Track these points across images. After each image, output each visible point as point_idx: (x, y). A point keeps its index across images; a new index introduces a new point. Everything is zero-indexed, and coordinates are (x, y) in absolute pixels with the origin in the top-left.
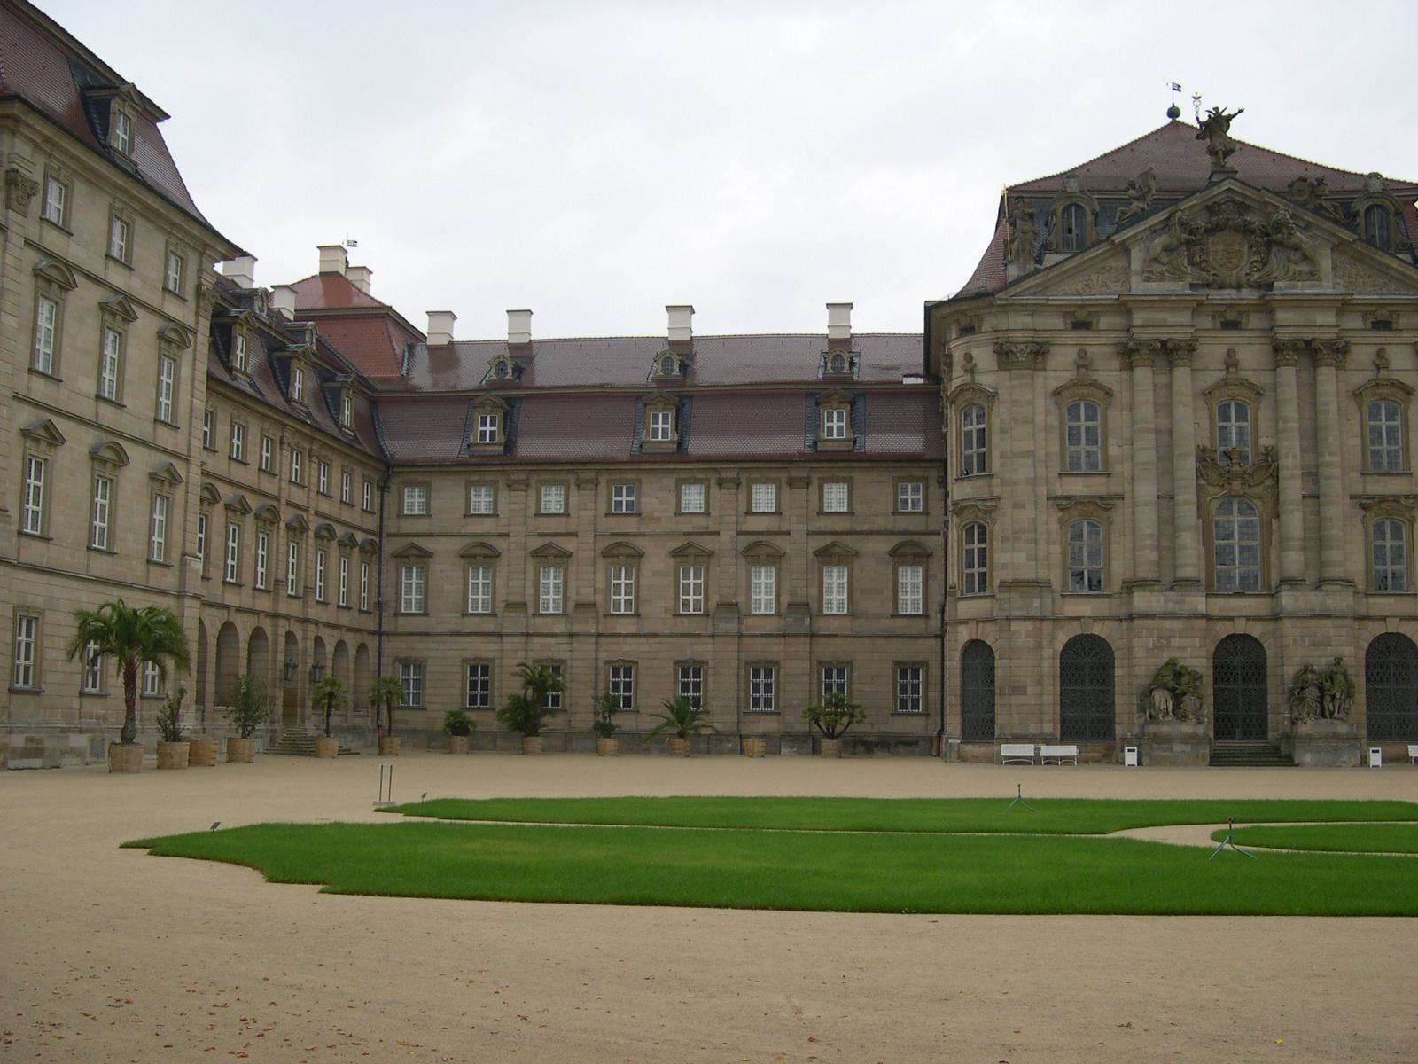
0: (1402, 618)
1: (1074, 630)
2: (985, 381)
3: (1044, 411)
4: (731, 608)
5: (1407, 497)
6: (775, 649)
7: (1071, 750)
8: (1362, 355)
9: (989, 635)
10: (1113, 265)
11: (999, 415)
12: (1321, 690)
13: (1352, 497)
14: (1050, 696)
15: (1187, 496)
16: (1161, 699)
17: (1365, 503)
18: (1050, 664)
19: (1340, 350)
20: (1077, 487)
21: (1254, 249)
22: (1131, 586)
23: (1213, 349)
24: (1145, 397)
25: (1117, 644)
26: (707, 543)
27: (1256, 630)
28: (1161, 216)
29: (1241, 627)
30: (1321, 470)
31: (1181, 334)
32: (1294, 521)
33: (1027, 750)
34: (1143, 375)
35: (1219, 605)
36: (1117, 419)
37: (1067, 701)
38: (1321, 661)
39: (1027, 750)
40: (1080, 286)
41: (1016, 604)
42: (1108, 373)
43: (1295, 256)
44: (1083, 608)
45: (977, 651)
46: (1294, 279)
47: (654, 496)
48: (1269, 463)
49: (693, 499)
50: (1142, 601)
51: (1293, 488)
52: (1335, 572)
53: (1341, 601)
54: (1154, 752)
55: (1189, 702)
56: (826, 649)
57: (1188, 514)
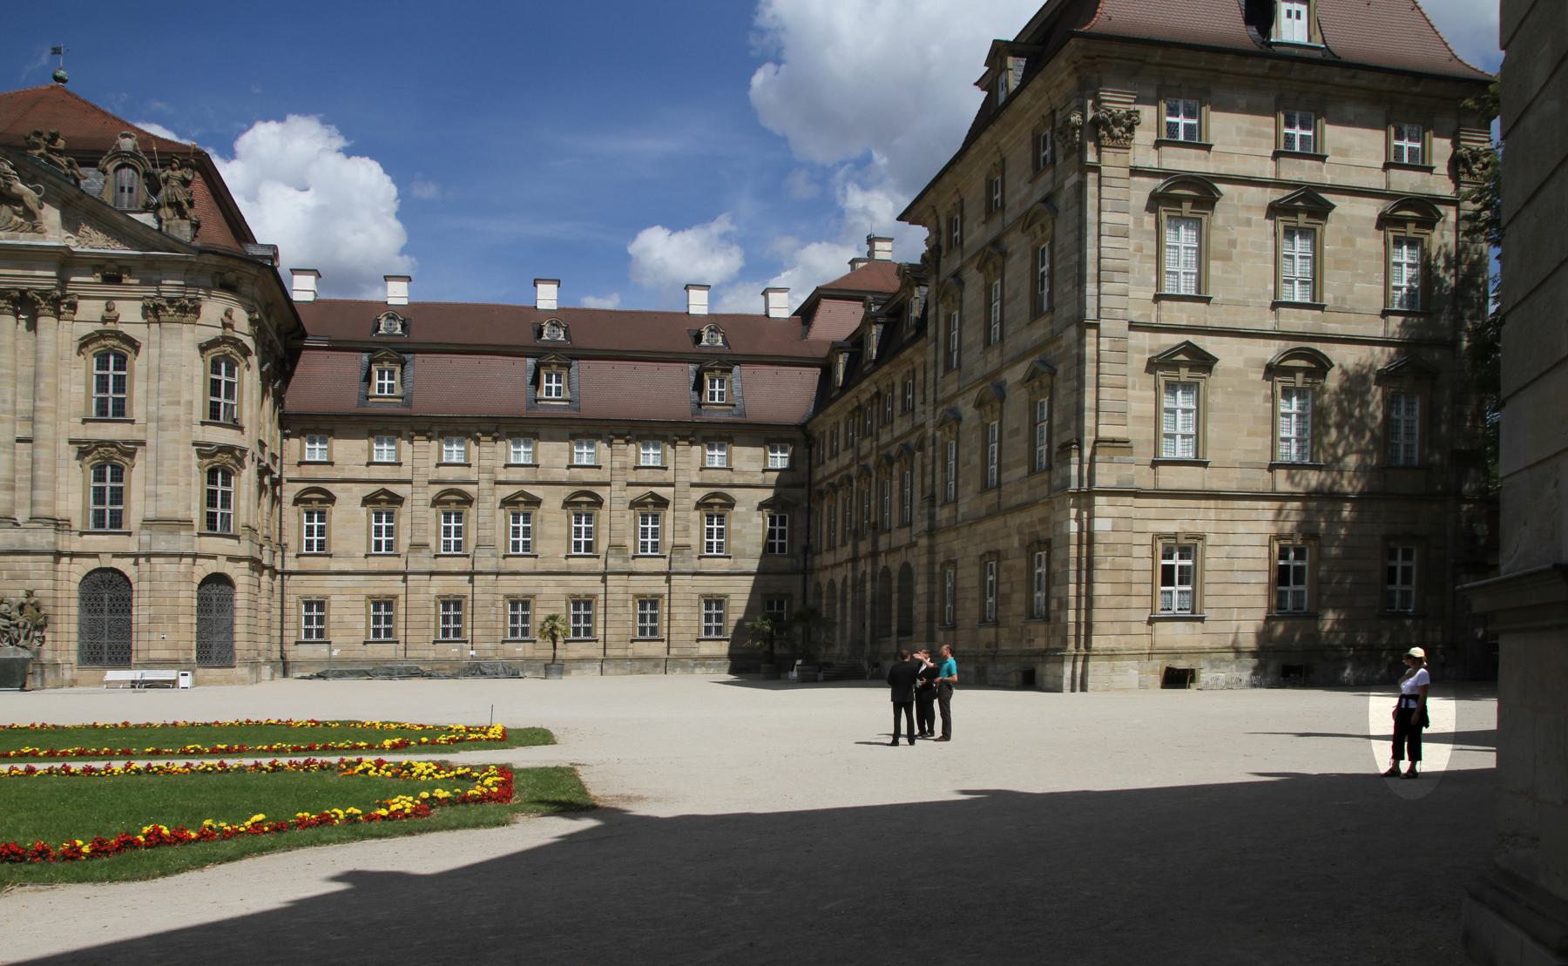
0: (115, 555)
5: (126, 442)
13: (71, 442)
17: (84, 449)
30: (37, 415)
52: (43, 511)
53: (44, 538)
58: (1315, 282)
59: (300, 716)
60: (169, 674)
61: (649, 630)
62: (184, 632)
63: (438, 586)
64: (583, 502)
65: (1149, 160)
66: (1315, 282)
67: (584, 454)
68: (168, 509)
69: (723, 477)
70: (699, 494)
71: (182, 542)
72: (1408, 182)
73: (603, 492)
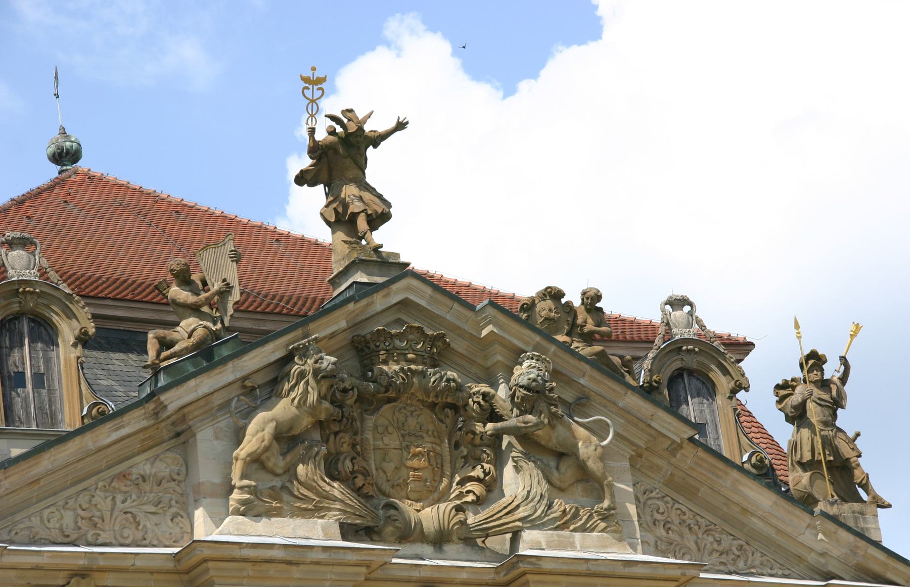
10: (147, 469)
21: (464, 451)
28: (270, 352)
40: (68, 519)
43: (568, 471)
46: (563, 527)
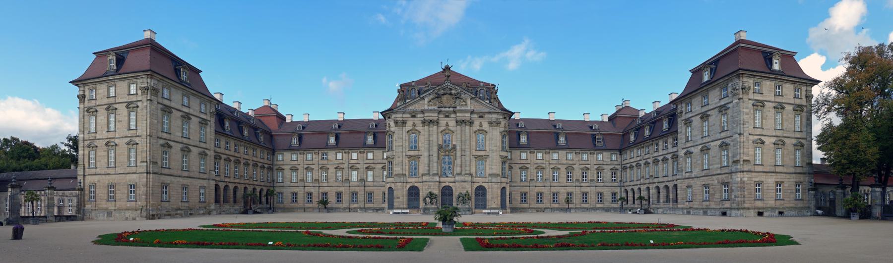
1: (411, 185)
2: (392, 129)
3: (405, 136)
4: (348, 180)
6: (357, 189)
7: (408, 211)
8: (477, 124)
9: (393, 186)
11: (395, 137)
12: (464, 198)
14: (405, 199)
15: (435, 155)
16: (428, 199)
18: (405, 192)
19: (471, 123)
20: (412, 153)
22: (423, 175)
23: (443, 122)
24: (427, 133)
25: (420, 188)
26: (342, 166)
27: (451, 185)
29: (447, 184)
31: (435, 119)
32: (458, 161)
33: (399, 211)
34: (426, 127)
35: (442, 179)
36: (422, 138)
37: (409, 200)
38: (464, 192)
39: (399, 211)
41: (397, 179)
42: (419, 127)
44: (413, 180)
45: (390, 188)
47: (331, 155)
48: (454, 147)
49: (339, 156)
50: (425, 178)
51: (459, 154)
53: (469, 178)
54: (426, 211)
55: (434, 200)
56: (368, 189)
57: (435, 159)
58: (782, 124)
59: (492, 222)
60: (497, 211)
61: (585, 200)
62: (497, 202)
63: (537, 189)
64: (570, 169)
65: (752, 97)
66: (782, 124)
67: (570, 156)
68: (494, 172)
69: (601, 162)
70: (596, 167)
71: (499, 179)
72: (798, 102)
73: (574, 166)
